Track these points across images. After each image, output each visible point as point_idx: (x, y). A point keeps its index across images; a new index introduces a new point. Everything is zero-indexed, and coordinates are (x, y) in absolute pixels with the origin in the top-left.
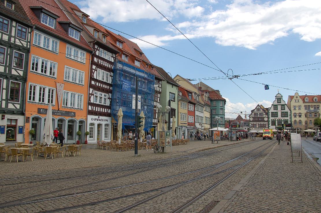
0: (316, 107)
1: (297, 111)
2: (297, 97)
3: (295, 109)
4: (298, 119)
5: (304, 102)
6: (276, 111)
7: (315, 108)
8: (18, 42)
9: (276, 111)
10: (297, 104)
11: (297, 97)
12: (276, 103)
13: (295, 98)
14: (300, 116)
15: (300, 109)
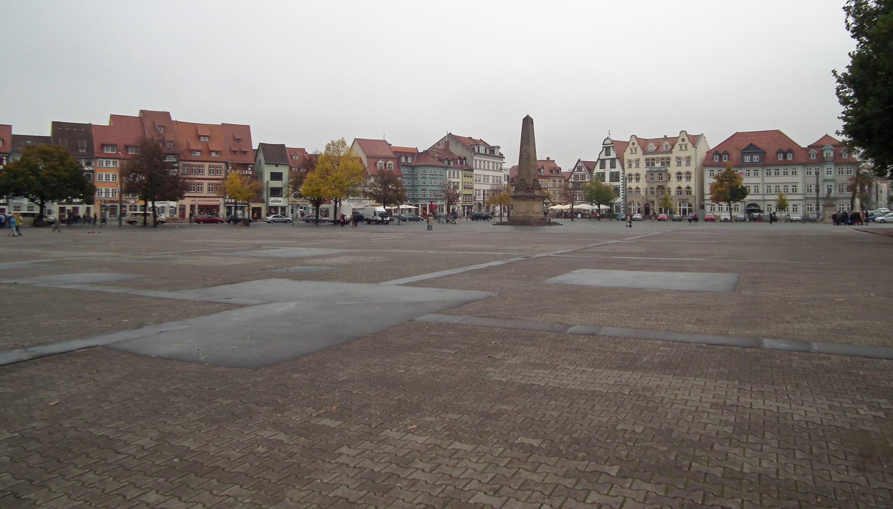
0: (665, 161)
1: (633, 171)
2: (633, 144)
3: (630, 166)
4: (684, 184)
5: (645, 152)
6: (602, 171)
7: (663, 164)
8: (86, 169)
9: (602, 171)
10: (633, 157)
11: (683, 140)
12: (603, 156)
13: (680, 141)
14: (689, 178)
15: (638, 166)
